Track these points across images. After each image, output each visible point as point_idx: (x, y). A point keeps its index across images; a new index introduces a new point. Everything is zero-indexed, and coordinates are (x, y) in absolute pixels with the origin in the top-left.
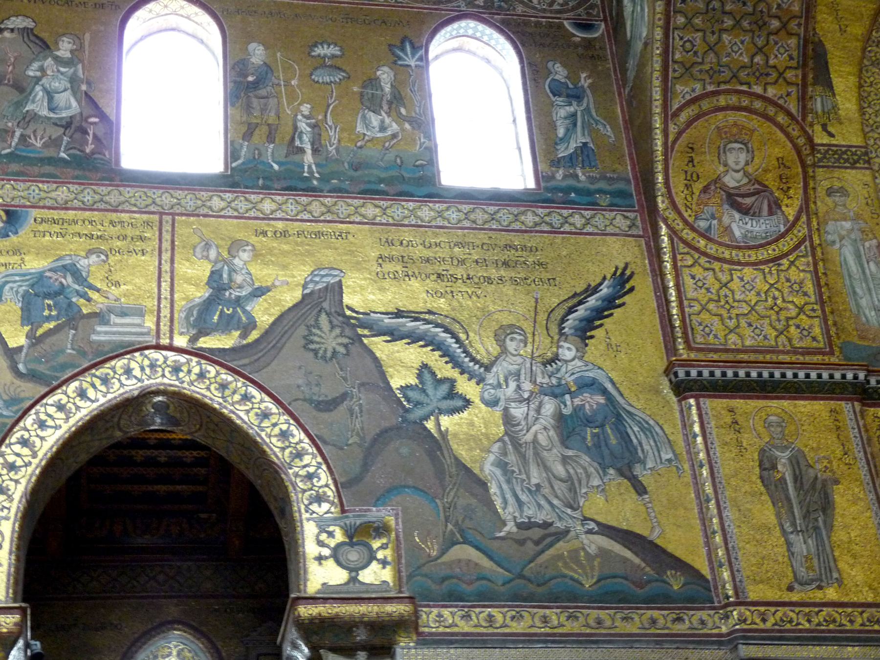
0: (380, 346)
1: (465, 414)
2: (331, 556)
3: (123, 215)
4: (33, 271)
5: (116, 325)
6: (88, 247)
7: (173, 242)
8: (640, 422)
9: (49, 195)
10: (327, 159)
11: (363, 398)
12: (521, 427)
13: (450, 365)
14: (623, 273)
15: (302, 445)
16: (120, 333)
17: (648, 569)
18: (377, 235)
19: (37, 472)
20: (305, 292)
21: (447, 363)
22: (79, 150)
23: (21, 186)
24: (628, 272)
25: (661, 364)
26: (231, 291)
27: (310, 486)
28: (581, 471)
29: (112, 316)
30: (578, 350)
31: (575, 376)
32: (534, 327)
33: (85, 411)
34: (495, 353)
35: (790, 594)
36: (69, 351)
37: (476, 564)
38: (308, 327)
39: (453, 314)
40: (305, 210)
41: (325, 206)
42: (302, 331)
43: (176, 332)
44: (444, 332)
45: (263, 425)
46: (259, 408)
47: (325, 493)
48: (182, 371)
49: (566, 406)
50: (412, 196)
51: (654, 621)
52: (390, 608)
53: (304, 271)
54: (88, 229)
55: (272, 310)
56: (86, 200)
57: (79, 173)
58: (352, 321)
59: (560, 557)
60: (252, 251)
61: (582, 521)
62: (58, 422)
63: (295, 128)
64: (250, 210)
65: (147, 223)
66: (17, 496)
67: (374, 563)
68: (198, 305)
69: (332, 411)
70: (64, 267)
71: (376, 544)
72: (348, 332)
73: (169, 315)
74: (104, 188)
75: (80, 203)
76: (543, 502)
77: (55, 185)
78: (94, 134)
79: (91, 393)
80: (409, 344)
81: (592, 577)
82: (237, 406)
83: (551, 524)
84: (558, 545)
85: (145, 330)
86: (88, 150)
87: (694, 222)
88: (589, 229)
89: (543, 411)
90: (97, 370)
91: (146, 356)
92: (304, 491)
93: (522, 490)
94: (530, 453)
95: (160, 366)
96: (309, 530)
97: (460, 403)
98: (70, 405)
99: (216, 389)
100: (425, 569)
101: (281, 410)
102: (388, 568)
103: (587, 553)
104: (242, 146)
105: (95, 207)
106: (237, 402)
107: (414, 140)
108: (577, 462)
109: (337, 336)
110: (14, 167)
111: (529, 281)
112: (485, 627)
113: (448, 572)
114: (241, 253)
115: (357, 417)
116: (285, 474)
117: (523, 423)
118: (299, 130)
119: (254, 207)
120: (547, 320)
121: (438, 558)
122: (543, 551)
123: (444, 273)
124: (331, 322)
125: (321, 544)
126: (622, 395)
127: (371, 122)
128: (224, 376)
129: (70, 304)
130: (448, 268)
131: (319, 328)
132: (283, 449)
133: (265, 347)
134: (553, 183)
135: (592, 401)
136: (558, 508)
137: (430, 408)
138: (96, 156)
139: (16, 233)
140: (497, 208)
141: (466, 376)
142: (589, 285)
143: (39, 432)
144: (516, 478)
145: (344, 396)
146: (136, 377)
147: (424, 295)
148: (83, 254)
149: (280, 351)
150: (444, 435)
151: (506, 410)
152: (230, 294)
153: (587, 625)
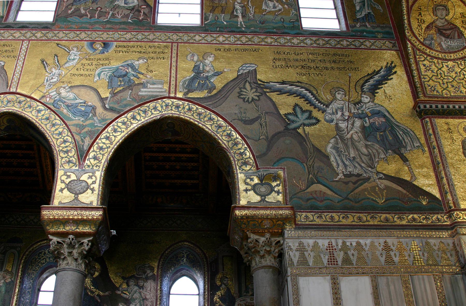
0: (274, 97)
1: (317, 126)
3: (155, 43)
4: (114, 67)
5: (150, 88)
7: (177, 54)
8: (403, 130)
9: (123, 36)
12: (345, 132)
13: (309, 105)
15: (238, 140)
16: (152, 92)
17: (410, 195)
19: (113, 151)
20: (239, 74)
21: (307, 103)
22: (136, 18)
24: (393, 65)
25: (411, 104)
28: (375, 151)
29: (149, 85)
30: (371, 98)
31: (370, 109)
32: (349, 88)
33: (135, 125)
37: (324, 193)
38: (240, 88)
39: (309, 83)
40: (239, 40)
41: (248, 38)
42: (237, 90)
43: (177, 91)
44: (305, 90)
45: (218, 131)
46: (217, 124)
47: (248, 161)
48: (180, 108)
49: (366, 122)
50: (289, 34)
55: (223, 81)
56: (139, 38)
57: (137, 27)
58: (261, 86)
59: (365, 190)
60: (214, 57)
61: (376, 173)
62: (123, 130)
63: (234, 8)
66: (103, 161)
69: (252, 124)
70: (128, 65)
71: (274, 184)
72: (259, 90)
74: (147, 33)
75: (136, 39)
76: (356, 165)
77: (125, 32)
78: (144, 12)
79: (138, 117)
81: (383, 200)
82: (206, 123)
83: (361, 175)
84: (365, 185)
85: (164, 90)
86: (140, 19)
88: (373, 47)
89: (355, 125)
90: (141, 107)
94: (350, 143)
95: (170, 106)
96: (241, 176)
97: (314, 121)
98: (128, 122)
99: (197, 115)
100: (299, 195)
102: (280, 195)
103: (379, 188)
104: (209, 15)
105: (143, 40)
106: (207, 121)
107: (290, 11)
108: (373, 147)
110: (108, 26)
111: (346, 69)
112: (329, 222)
113: (311, 197)
114: (208, 58)
115: (264, 127)
116: (229, 153)
117: (346, 130)
118: (236, 8)
120: (355, 85)
121: (304, 190)
122: (357, 187)
124: (251, 86)
125: (247, 184)
126: (393, 118)
127: (269, 5)
128: (200, 110)
129: (130, 80)
130: (307, 63)
131: (245, 89)
133: (220, 97)
134: (355, 29)
135: (378, 121)
136: (364, 168)
140: (329, 39)
141: (317, 109)
142: (375, 71)
143: (114, 134)
144: (343, 154)
146: (159, 110)
148: (137, 59)
149: (227, 99)
151: (337, 124)
152: (203, 75)
153: (381, 221)
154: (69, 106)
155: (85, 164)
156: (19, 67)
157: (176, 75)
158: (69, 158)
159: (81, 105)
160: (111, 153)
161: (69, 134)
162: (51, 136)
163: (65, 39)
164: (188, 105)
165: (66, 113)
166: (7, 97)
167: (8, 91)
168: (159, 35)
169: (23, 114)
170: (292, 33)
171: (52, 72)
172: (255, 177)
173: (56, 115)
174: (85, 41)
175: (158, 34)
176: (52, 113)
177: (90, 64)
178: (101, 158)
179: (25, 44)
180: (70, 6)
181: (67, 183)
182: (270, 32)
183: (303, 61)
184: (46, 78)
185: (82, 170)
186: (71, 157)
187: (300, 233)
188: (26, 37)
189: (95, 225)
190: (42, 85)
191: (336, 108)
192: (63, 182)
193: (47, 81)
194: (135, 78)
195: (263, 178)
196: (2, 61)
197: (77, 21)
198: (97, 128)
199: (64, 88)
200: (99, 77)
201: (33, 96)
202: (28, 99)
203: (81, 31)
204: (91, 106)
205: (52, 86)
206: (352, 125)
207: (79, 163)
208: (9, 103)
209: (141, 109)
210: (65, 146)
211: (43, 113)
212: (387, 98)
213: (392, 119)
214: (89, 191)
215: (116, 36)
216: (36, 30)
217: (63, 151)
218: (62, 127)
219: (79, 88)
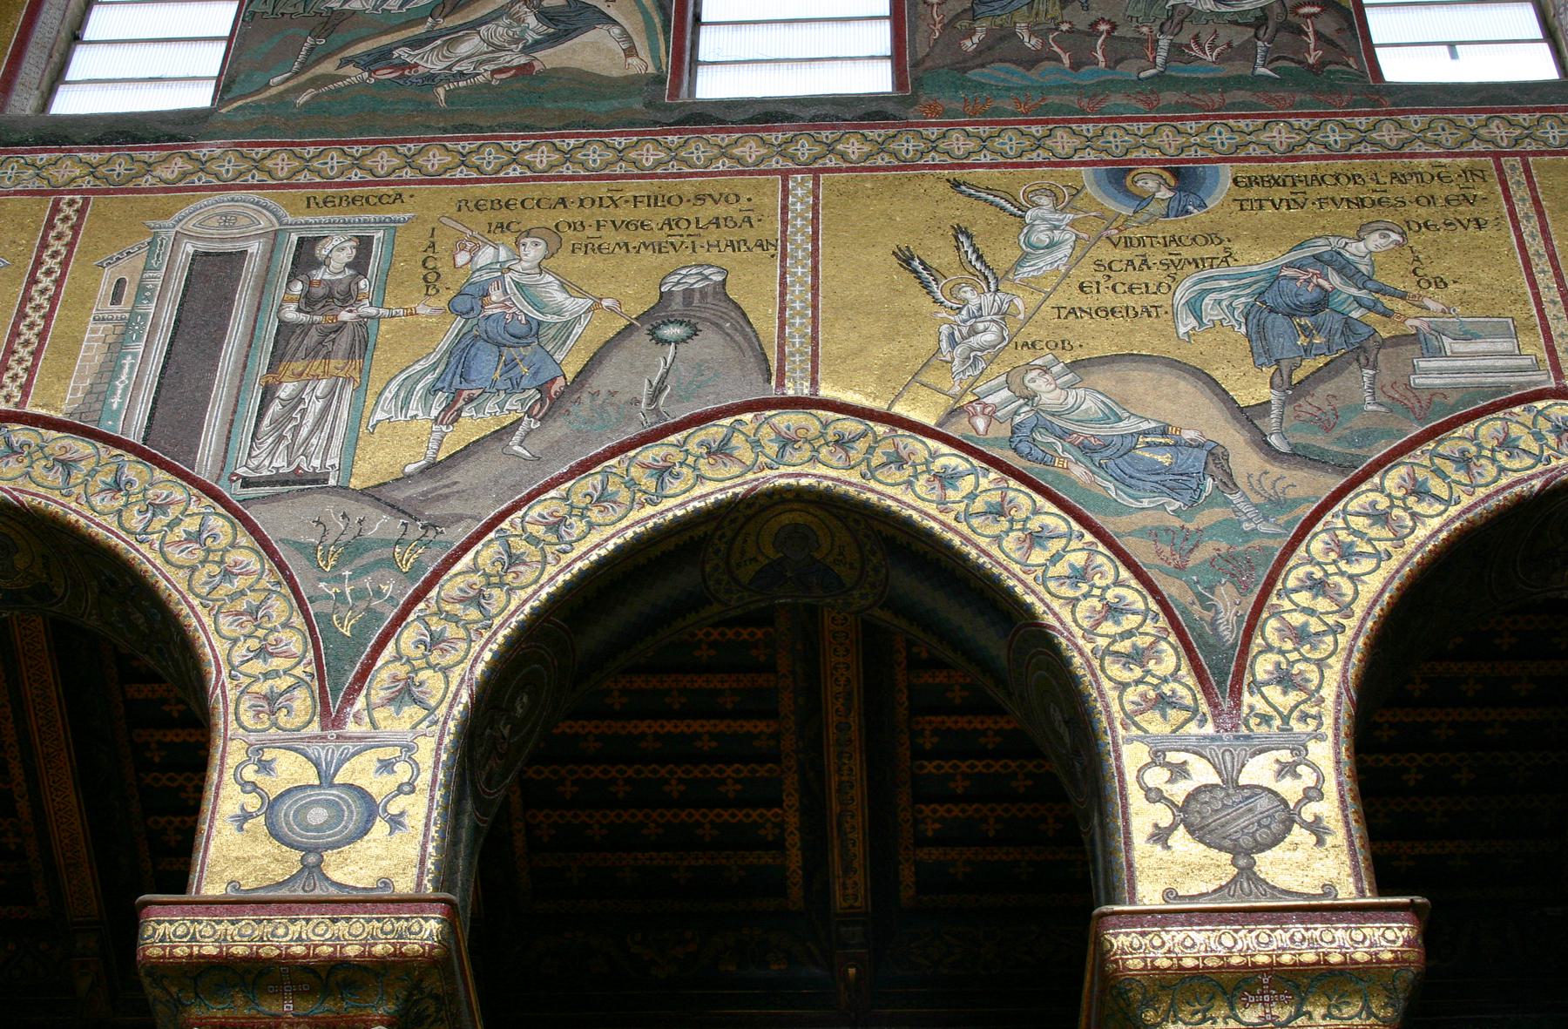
3: (1416, 161)
4: (1255, 268)
5: (1456, 355)
6: (1359, 222)
7: (1536, 202)
16: (1472, 371)
19: (1361, 642)
22: (1292, 60)
23: (1191, 126)
29: (1447, 341)
36: (1370, 408)
54: (1351, 191)
56: (1331, 139)
57: (1308, 98)
62: (1381, 546)
66: (1329, 692)
74: (1363, 119)
75: (1321, 149)
77: (1260, 121)
78: (1316, 33)
79: (1437, 487)
85: (1528, 362)
90: (1439, 443)
98: (1396, 512)
105: (1353, 151)
110: (1169, 97)
129: (1348, 322)
139: (1203, 205)
143: (1343, 565)
148: (1353, 233)
154: (1094, 451)
155: (1245, 710)
156: (797, 288)
158: (1156, 687)
159: (1149, 445)
160: (1356, 656)
161: (1125, 574)
162: (1040, 589)
163: (983, 161)
165: (1085, 479)
166: (774, 420)
167: (772, 392)
169: (874, 498)
171: (965, 302)
173: (1035, 495)
174: (1084, 164)
175: (1416, 121)
176: (1013, 483)
177: (1137, 263)
178: (1314, 676)
179: (800, 188)
180: (965, 23)
181: (1179, 799)
184: (945, 329)
185: (1237, 738)
186: (1165, 680)
188: (793, 158)
189: (1390, 992)
190: (934, 362)
192: (1154, 796)
193: (953, 343)
194: (1372, 315)
196: (710, 266)
197: (1016, 81)
198: (1256, 542)
199: (1045, 370)
200: (1199, 318)
201: (900, 409)
202: (881, 429)
203: (1047, 122)
204: (1200, 446)
205: (982, 365)
207: (1214, 705)
208: (789, 449)
209: (1440, 449)
210: (1119, 630)
211: (967, 484)
214: (1298, 834)
215: (1222, 137)
216: (833, 127)
217: (1116, 653)
218: (1080, 545)
219: (1116, 367)
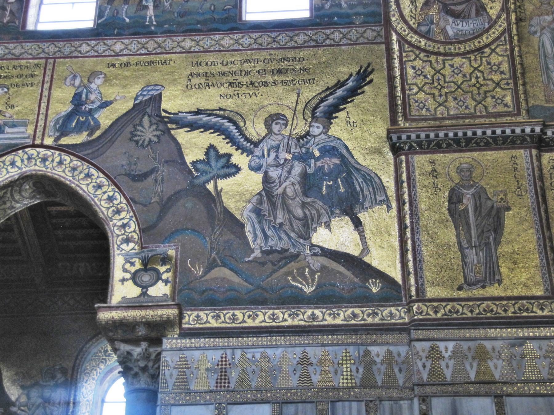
2: (131, 278)
3: (22, 61)
5: (8, 133)
7: (52, 76)
10: (163, 11)
11: (164, 171)
12: (275, 184)
13: (230, 144)
14: (366, 70)
15: (122, 205)
16: (10, 139)
18: (190, 60)
20: (136, 102)
21: (227, 143)
24: (370, 69)
26: (87, 106)
27: (123, 232)
28: (315, 212)
29: (6, 128)
30: (324, 128)
31: (320, 146)
32: (294, 114)
34: (264, 135)
35: (460, 293)
38: (135, 126)
41: (157, 43)
42: (130, 128)
43: (46, 135)
47: (132, 236)
48: (48, 160)
49: (310, 167)
50: (219, 30)
51: (355, 316)
52: (160, 312)
53: (137, 88)
58: (166, 120)
60: (104, 78)
64: (106, 50)
65: (37, 65)
67: (160, 282)
68: (63, 116)
69: (142, 181)
71: (162, 269)
72: (161, 127)
73: (43, 125)
76: (283, 235)
80: (202, 132)
81: (312, 287)
82: (81, 182)
83: (287, 250)
84: (290, 265)
86: (5, 21)
87: (417, 28)
89: (293, 172)
91: (26, 153)
92: (118, 236)
93: (269, 227)
95: (34, 158)
99: (69, 171)
101: (110, 183)
102: (169, 285)
103: (310, 269)
104: (106, 8)
105: (5, 57)
106: (82, 179)
108: (312, 206)
109: (154, 130)
112: (229, 323)
114: (96, 80)
115: (160, 184)
117: (277, 181)
119: (109, 49)
123: (235, 81)
124: (150, 121)
126: (353, 157)
128: (75, 162)
130: (238, 78)
131: (143, 126)
132: (108, 209)
134: (322, 12)
137: (212, 175)
138: (10, 24)
141: (240, 151)
142: (339, 81)
144: (266, 220)
145: (153, 171)
146: (18, 167)
147: (218, 98)
149: (113, 143)
150: (219, 193)
157: (47, 111)
164: (60, 155)
168: (29, 48)
170: (224, 29)
172: (137, 260)
175: (27, 46)
182: (191, 31)
183: (232, 74)
187: (186, 342)
191: (269, 146)
195: (148, 261)
206: (288, 172)
212: (349, 125)
213: (350, 159)
